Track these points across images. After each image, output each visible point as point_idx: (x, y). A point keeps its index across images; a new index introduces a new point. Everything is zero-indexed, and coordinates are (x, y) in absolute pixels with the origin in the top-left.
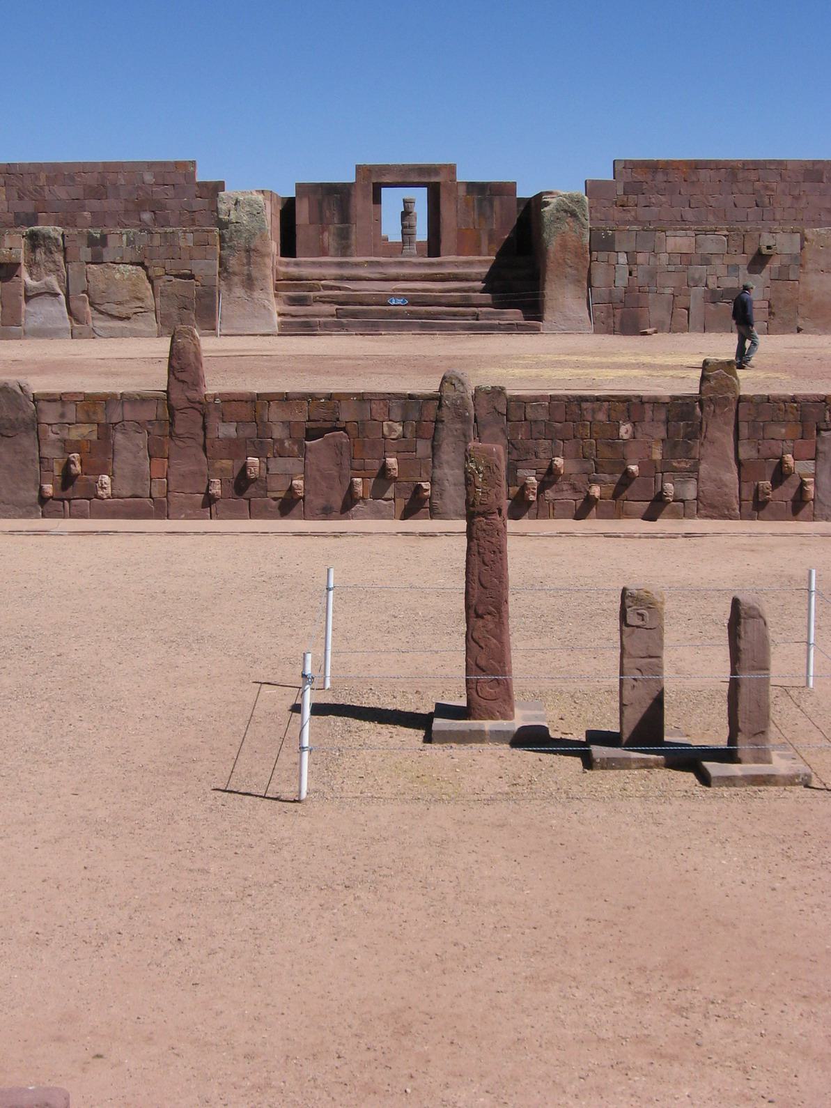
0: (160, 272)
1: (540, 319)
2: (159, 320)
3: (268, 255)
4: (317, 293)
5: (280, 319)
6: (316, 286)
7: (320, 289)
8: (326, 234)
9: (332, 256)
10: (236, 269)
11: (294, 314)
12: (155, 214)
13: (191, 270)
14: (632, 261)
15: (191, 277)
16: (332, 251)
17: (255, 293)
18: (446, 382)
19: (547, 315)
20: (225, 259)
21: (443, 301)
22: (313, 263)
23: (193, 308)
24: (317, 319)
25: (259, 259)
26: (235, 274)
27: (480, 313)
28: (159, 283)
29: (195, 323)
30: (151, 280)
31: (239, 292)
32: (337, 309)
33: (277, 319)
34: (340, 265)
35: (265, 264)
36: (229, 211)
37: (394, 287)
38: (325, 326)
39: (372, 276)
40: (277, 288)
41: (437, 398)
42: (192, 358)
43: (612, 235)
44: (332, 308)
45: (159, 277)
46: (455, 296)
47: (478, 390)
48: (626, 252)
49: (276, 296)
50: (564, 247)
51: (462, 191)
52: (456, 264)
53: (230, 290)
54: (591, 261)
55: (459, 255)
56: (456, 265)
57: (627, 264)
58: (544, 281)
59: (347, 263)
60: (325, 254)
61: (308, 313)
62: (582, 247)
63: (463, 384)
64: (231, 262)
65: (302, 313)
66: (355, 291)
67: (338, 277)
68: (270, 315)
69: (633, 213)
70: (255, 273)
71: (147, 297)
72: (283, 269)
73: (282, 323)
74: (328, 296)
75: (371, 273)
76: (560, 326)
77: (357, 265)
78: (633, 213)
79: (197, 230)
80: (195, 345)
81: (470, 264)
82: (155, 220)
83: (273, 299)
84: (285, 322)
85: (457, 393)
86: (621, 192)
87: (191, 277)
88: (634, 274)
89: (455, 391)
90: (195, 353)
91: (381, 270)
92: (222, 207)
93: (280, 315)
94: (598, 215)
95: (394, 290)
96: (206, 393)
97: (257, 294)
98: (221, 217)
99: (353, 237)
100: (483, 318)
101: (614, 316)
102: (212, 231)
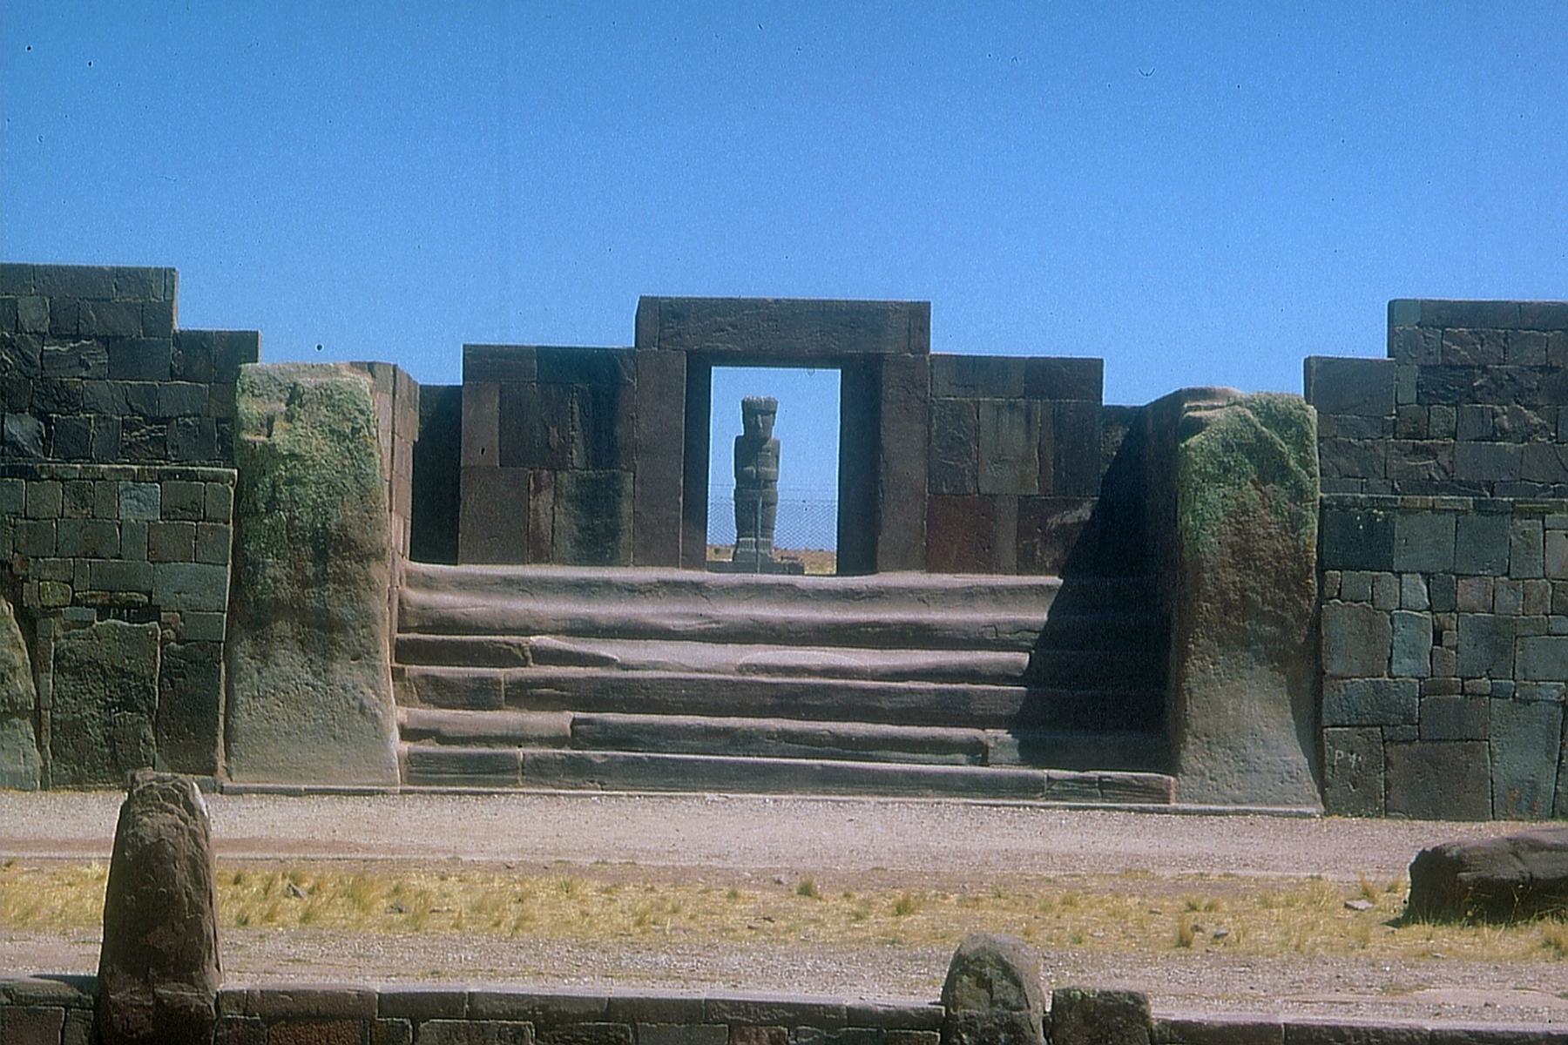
0: (55, 595)
1: (1168, 762)
2: (47, 740)
3: (379, 555)
4: (518, 672)
5: (406, 747)
6: (517, 652)
7: (526, 659)
8: (547, 497)
9: (562, 562)
10: (285, 592)
11: (446, 730)
12: (48, 422)
13: (149, 594)
14: (1442, 596)
15: (150, 612)
16: (566, 546)
17: (337, 666)
18: (965, 971)
19: (1191, 756)
20: (255, 564)
21: (885, 703)
22: (508, 582)
23: (151, 709)
24: (519, 752)
25: (352, 567)
26: (280, 608)
27: (991, 744)
28: (54, 629)
29: (154, 751)
30: (27, 619)
31: (289, 663)
33: (399, 747)
34: (583, 589)
35: (369, 580)
36: (270, 421)
37: (741, 661)
38: (538, 771)
39: (678, 624)
40: (403, 652)
41: (941, 1024)
42: (182, 875)
43: (1386, 521)
45: (55, 611)
46: (921, 692)
47: (1065, 1003)
48: (1427, 576)
49: (397, 675)
50: (1243, 555)
53: (265, 657)
54: (1322, 598)
55: (931, 566)
57: (1429, 609)
58: (1184, 654)
59: (608, 584)
60: (540, 557)
62: (1298, 555)
63: (1018, 983)
64: (270, 571)
65: (472, 731)
66: (624, 667)
67: (579, 626)
68: (380, 735)
69: (1444, 458)
70: (340, 609)
71: (13, 670)
72: (416, 596)
73: (411, 760)
74: (550, 682)
76: (1228, 791)
77: (632, 590)
78: (1444, 458)
79: (171, 474)
80: (193, 834)
81: (969, 596)
82: (49, 440)
83: (389, 687)
84: (420, 755)
85: (998, 1009)
86: (1408, 395)
87: (150, 612)
88: (1449, 638)
89: (993, 1003)
90: (193, 860)
91: (705, 608)
92: (249, 407)
93: (407, 734)
94: (1342, 461)
95: (742, 669)
96: (221, 987)
97: (343, 670)
98: (247, 437)
99: (626, 508)
101: (1388, 761)
102: (217, 478)
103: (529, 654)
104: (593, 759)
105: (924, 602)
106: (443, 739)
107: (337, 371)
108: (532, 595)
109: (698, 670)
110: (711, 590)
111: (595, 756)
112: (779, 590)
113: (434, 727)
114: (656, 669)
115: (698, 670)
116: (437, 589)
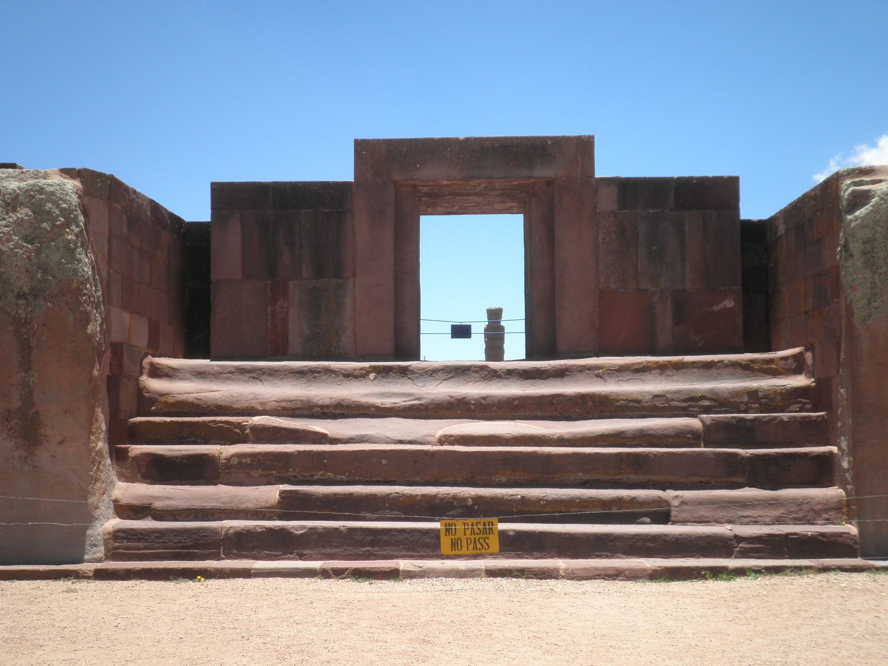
11: (158, 504)
22: (243, 371)
27: (676, 503)
32: (282, 493)
39: (388, 402)
44: (271, 493)
49: (119, 456)
51: (607, 201)
52: (601, 374)
56: (598, 376)
59: (328, 371)
61: (198, 504)
75: (383, 395)
77: (349, 376)
100: (685, 515)
103: (248, 431)
104: (293, 531)
105: (601, 377)
106: (159, 515)
107: (46, 176)
108: (261, 381)
109: (401, 442)
110: (415, 373)
111: (293, 527)
112: (473, 371)
113: (146, 502)
114: (366, 442)
115: (401, 442)
116: (182, 379)
